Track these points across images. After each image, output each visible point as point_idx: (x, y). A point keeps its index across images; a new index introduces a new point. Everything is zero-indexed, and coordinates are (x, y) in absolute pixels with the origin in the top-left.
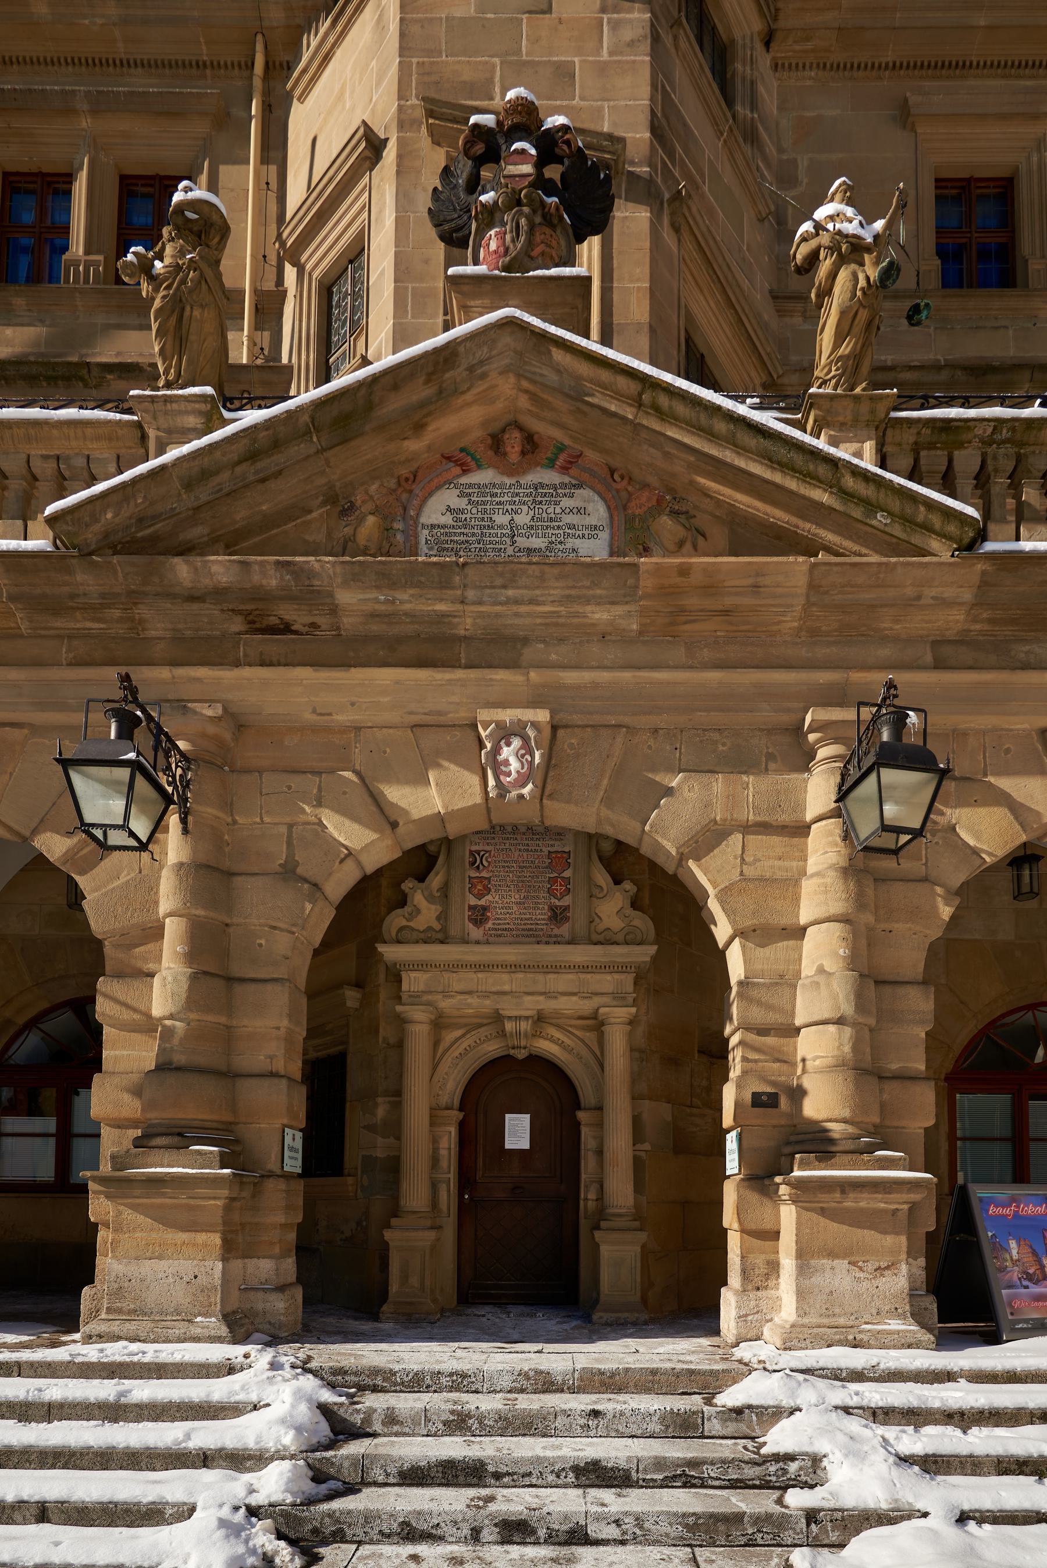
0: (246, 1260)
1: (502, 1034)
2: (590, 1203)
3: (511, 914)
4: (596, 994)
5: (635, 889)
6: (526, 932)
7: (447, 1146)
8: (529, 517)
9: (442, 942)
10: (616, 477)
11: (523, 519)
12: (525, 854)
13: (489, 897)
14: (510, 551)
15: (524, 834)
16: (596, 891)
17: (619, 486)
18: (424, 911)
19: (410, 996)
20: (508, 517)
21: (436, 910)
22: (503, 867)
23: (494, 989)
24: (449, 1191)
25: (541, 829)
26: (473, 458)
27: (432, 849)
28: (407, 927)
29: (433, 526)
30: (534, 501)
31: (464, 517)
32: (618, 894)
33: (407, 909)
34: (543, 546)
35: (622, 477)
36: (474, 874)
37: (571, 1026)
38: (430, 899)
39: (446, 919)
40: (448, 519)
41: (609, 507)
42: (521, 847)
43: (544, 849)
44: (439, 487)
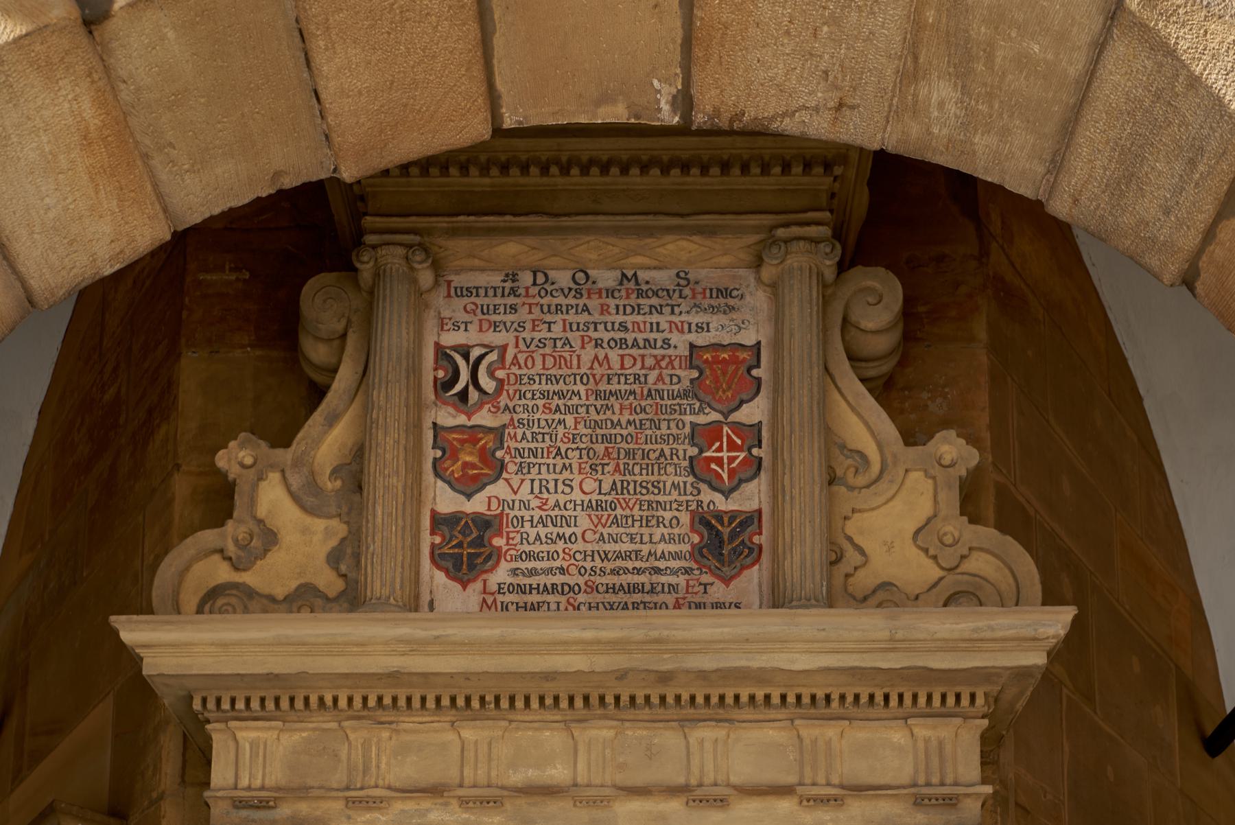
3: (571, 539)
4: (859, 790)
6: (621, 597)
12: (614, 356)
13: (499, 489)
15: (611, 293)
16: (843, 465)
18: (289, 537)
21: (328, 532)
22: (545, 395)
23: (517, 778)
28: (235, 586)
39: (357, 557)
42: (602, 334)
43: (675, 338)
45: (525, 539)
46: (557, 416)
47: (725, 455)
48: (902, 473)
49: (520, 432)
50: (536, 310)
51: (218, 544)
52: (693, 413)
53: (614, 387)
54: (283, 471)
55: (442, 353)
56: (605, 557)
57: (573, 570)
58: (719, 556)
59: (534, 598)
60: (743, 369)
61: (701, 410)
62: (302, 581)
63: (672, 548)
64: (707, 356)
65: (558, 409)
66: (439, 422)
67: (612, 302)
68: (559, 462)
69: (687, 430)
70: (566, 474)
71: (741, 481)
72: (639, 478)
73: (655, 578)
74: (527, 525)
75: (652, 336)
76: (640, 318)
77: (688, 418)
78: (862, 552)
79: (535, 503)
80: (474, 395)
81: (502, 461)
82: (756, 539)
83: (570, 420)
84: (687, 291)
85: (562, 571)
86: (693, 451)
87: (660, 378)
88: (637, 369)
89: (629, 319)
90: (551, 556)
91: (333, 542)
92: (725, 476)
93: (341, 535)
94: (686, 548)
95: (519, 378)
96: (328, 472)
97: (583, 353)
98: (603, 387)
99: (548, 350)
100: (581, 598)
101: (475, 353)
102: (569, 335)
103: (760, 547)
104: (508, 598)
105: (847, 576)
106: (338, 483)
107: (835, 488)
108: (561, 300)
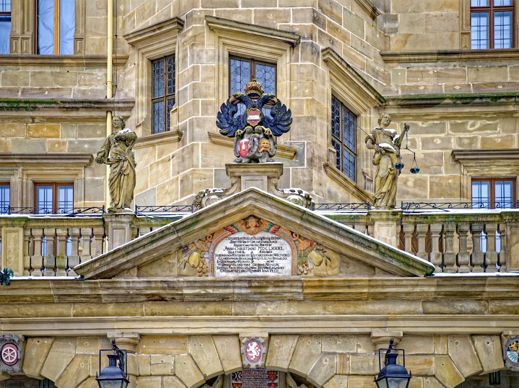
8: (259, 251)
10: (294, 235)
11: (256, 252)
14: (251, 265)
17: (295, 239)
20: (250, 251)
26: (237, 229)
29: (220, 255)
30: (261, 245)
31: (232, 251)
34: (265, 263)
35: (296, 235)
40: (226, 252)
41: (291, 247)
44: (222, 239)
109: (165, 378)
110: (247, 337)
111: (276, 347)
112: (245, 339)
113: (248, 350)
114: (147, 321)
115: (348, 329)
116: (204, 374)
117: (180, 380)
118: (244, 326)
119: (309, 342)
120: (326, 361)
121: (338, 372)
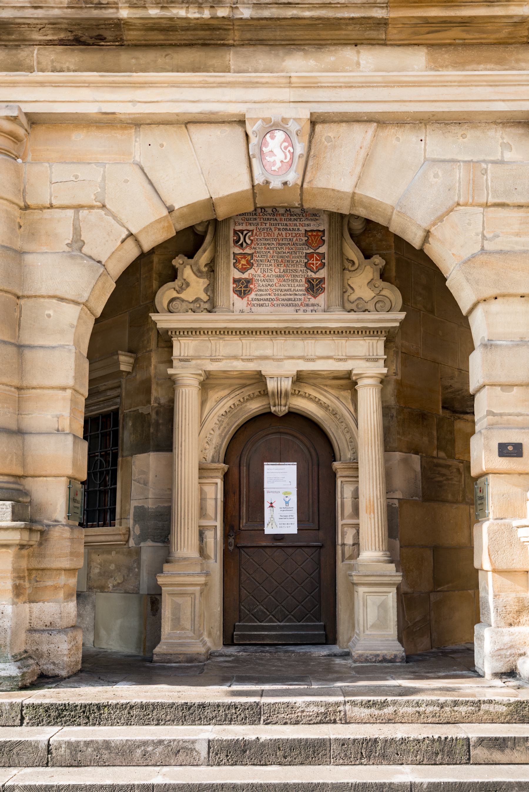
0: (32, 605)
1: (264, 393)
2: (346, 548)
3: (272, 286)
5: (384, 262)
6: (286, 302)
7: (214, 497)
9: (210, 312)
13: (252, 271)
15: (283, 215)
16: (348, 265)
18: (193, 284)
19: (181, 360)
21: (204, 283)
22: (264, 244)
24: (216, 538)
25: (298, 211)
27: (200, 229)
28: (178, 298)
32: (368, 267)
33: (177, 283)
36: (237, 250)
37: (326, 386)
38: (199, 273)
39: (213, 291)
43: (301, 228)
45: (259, 286)
46: (268, 250)
47: (315, 262)
48: (363, 267)
49: (257, 255)
50: (262, 220)
51: (173, 286)
52: (306, 250)
53: (284, 242)
54: (191, 266)
55: (235, 232)
56: (281, 291)
57: (272, 294)
58: (313, 291)
59: (262, 302)
60: (320, 238)
61: (308, 249)
62: (196, 297)
63: (300, 288)
64: (310, 234)
65: (268, 248)
66: (235, 252)
67: (283, 218)
68: (268, 263)
69: (304, 254)
70: (271, 267)
71: (319, 269)
72: (291, 268)
73: (295, 297)
74: (260, 281)
75: (294, 227)
76: (291, 222)
77: (304, 251)
78: (352, 288)
79: (262, 275)
80: (244, 245)
81: (252, 263)
82: (323, 286)
83: (271, 251)
84: (304, 215)
85: (269, 294)
86: (306, 261)
87: (297, 240)
88: (290, 237)
89: (288, 222)
90: (266, 291)
91: (205, 286)
92: (315, 268)
93: (208, 283)
94: (304, 288)
95: (257, 239)
96: (204, 265)
97: (275, 232)
98: (281, 242)
99: (265, 231)
100: (275, 302)
101: (245, 232)
102: (271, 227)
103: (324, 288)
104: (255, 302)
105: (348, 296)
106: (206, 269)
107: (345, 271)
108: (269, 217)
109: (83, 213)
110: (264, 120)
111: (326, 147)
112: (260, 122)
113: (264, 149)
114: (42, 84)
115: (486, 104)
116: (168, 205)
117: (115, 217)
118: (256, 99)
119: (398, 139)
120: (436, 176)
121: (461, 201)
